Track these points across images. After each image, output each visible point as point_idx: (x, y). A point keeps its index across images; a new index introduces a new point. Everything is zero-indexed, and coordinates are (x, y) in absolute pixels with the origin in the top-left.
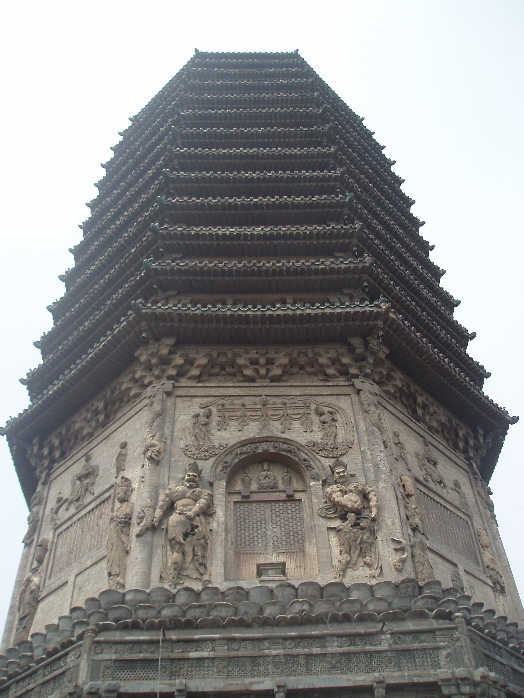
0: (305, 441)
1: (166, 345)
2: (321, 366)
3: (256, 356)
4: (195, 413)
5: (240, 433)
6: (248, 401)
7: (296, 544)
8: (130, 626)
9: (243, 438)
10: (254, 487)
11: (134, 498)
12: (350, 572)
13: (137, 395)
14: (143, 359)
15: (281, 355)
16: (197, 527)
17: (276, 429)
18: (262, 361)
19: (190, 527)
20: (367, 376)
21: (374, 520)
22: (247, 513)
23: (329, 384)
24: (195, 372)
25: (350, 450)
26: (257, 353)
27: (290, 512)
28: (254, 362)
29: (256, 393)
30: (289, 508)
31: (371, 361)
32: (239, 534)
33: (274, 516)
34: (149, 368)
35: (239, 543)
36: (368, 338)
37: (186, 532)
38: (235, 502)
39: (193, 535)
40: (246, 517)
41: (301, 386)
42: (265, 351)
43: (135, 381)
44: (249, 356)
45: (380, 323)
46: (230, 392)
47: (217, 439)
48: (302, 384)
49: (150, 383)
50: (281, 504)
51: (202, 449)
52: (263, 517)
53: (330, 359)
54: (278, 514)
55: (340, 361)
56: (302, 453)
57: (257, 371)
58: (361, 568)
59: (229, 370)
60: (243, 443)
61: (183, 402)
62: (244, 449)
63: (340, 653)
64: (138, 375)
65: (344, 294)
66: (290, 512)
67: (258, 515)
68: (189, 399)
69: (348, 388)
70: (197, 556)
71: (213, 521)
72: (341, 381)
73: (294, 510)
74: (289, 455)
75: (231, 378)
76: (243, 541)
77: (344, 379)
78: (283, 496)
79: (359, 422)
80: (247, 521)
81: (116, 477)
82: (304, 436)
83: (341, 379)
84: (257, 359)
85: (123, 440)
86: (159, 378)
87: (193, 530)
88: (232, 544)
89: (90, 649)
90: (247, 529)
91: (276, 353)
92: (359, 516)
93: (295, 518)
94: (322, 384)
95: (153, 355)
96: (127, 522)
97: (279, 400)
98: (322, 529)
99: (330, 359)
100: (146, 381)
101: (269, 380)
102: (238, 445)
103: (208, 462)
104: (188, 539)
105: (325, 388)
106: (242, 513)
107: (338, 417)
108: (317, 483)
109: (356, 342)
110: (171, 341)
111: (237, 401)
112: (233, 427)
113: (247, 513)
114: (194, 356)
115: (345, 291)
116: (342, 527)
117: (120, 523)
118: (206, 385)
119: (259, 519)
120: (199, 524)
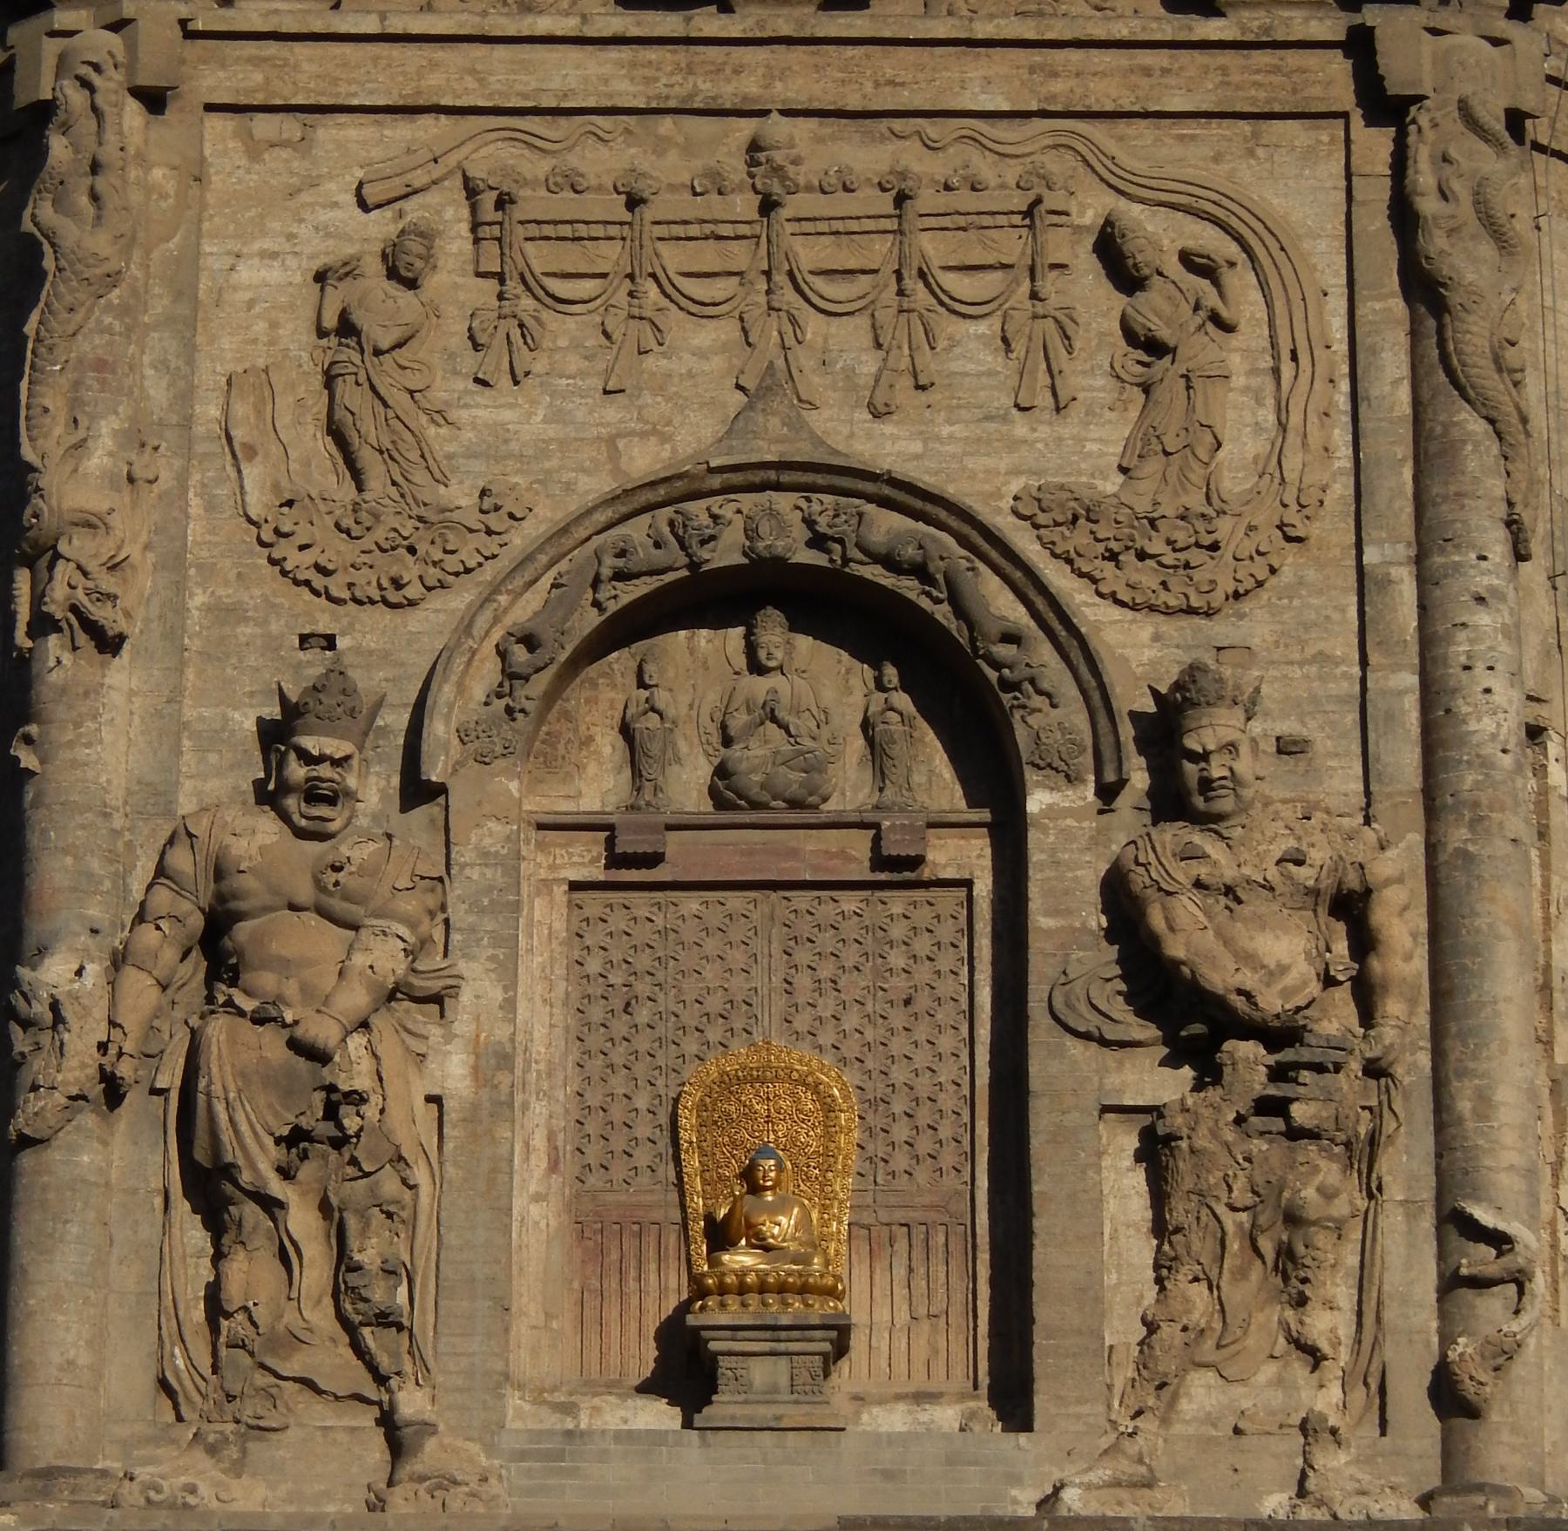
0: (1015, 486)
5: (612, 413)
6: (670, 161)
7: (922, 1176)
10: (687, 783)
16: (357, 1098)
19: (319, 1097)
22: (644, 961)
29: (728, 92)
32: (594, 1099)
33: (803, 981)
35: (594, 1153)
38: (575, 886)
40: (643, 987)
46: (556, 83)
47: (471, 455)
51: (380, 534)
52: (738, 984)
56: (995, 581)
58: (1270, 1370)
60: (634, 500)
61: (254, 150)
62: (636, 531)
66: (897, 959)
67: (710, 972)
68: (289, 126)
70: (357, 1268)
71: (449, 1037)
73: (923, 945)
74: (909, 587)
76: (619, 1142)
79: (1374, 351)
80: (643, 1014)
82: (1013, 444)
88: (554, 1167)
90: (640, 1069)
92: (1287, 1055)
93: (923, 1001)
97: (866, 156)
98: (1074, 1118)
102: (602, 517)
103: (414, 621)
104: (306, 1171)
106: (616, 956)
107: (1245, 300)
111: (603, 159)
112: (574, 363)
113: (644, 961)
119: (715, 1003)
120: (362, 1081)
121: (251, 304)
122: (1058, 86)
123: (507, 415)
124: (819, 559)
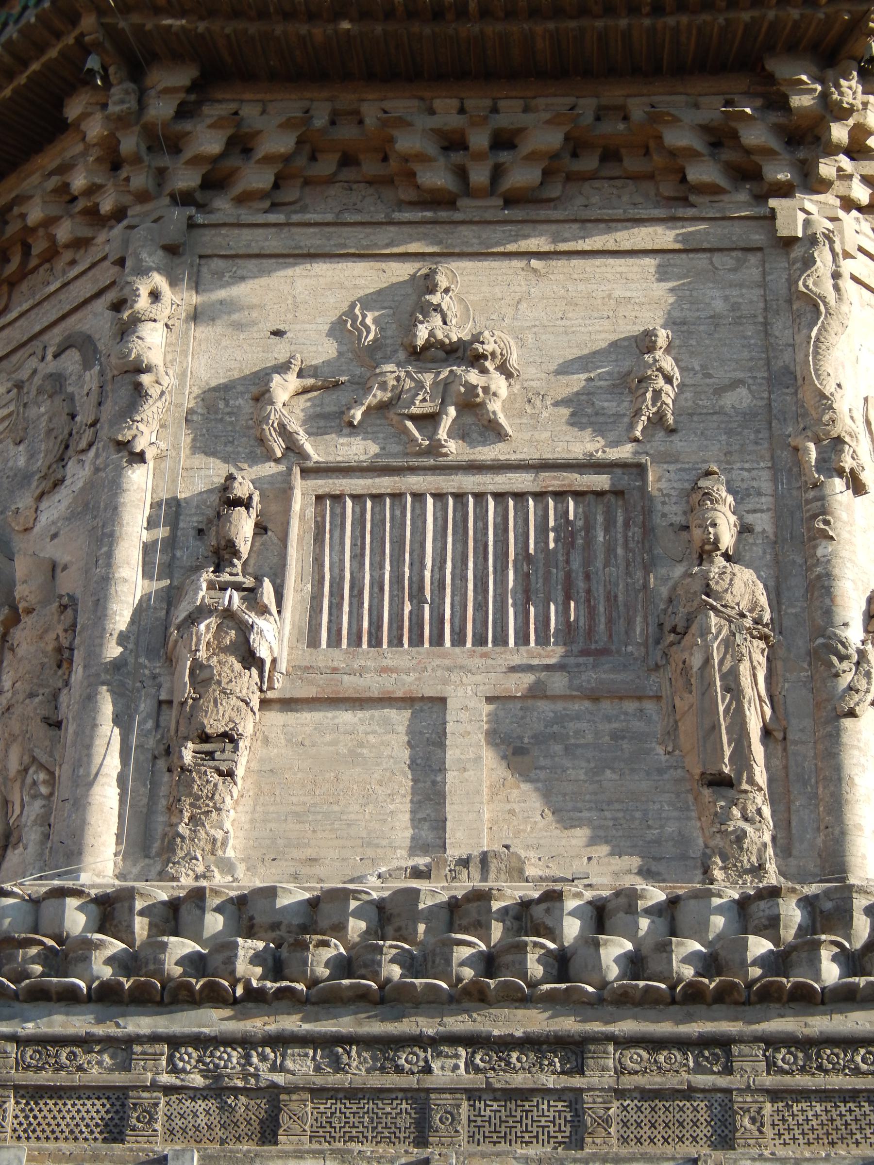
2: (673, 153)
14: (95, 129)
18: (479, 140)
28: (452, 143)
42: (488, 102)
53: (706, 129)
55: (735, 136)
57: (462, 173)
59: (371, 167)
64: (79, 182)
86: (143, 197)
91: (526, 110)
95: (122, 121)
99: (706, 129)
101: (500, 202)
118: (295, 218)
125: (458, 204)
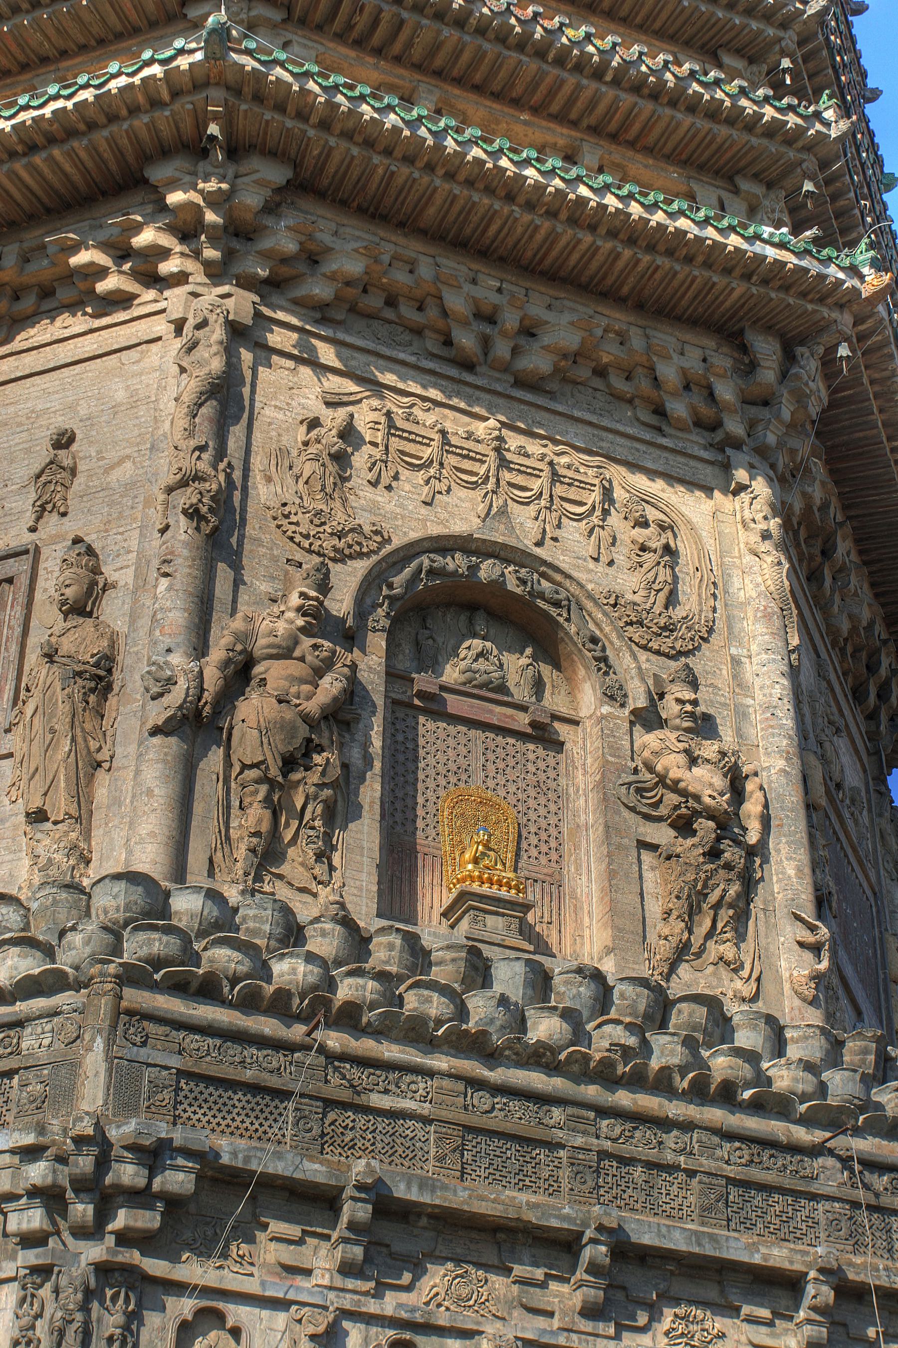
1: (260, 183)
3: (495, 298)
4: (311, 415)
5: (424, 510)
8: (195, 985)
9: (435, 530)
11: (114, 611)
12: (684, 971)
13: (122, 300)
15: (566, 318)
17: (524, 526)
18: (511, 320)
20: (762, 451)
21: (751, 852)
23: (664, 441)
24: (319, 289)
25: (704, 646)
26: (500, 290)
27: (531, 768)
30: (532, 756)
31: (786, 415)
33: (491, 767)
34: (187, 230)
36: (799, 350)
37: (292, 754)
39: (307, 769)
41: (590, 424)
43: (122, 252)
44: (478, 292)
45: (846, 320)
48: (594, 419)
49: (181, 278)
50: (511, 741)
53: (684, 372)
54: (501, 765)
57: (486, 342)
58: (711, 968)
63: (728, 1178)
65: (736, 191)
66: (531, 768)
69: (709, 470)
71: (353, 740)
72: (695, 443)
75: (407, 337)
77: (702, 441)
78: (522, 721)
81: (33, 530)
82: (590, 571)
83: (694, 438)
84: (496, 308)
85: (61, 422)
87: (307, 755)
89: (114, 1027)
91: (549, 307)
94: (647, 437)
96: (100, 678)
98: (626, 841)
99: (684, 372)
100: (167, 267)
105: (651, 450)
108: (619, 712)
109: (766, 349)
110: (276, 174)
114: (326, 238)
115: (745, 185)
116: (679, 850)
117: (79, 674)
119: (452, 766)
121: (270, 424)
122: (604, 444)
123: (380, 499)
124: (518, 591)
125: (478, 369)
